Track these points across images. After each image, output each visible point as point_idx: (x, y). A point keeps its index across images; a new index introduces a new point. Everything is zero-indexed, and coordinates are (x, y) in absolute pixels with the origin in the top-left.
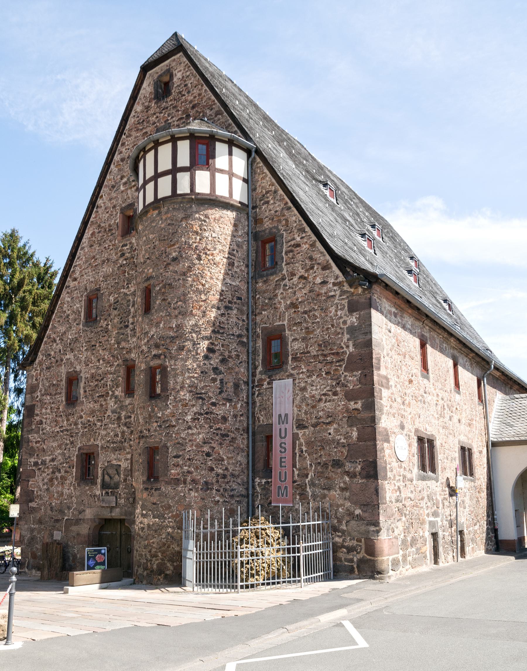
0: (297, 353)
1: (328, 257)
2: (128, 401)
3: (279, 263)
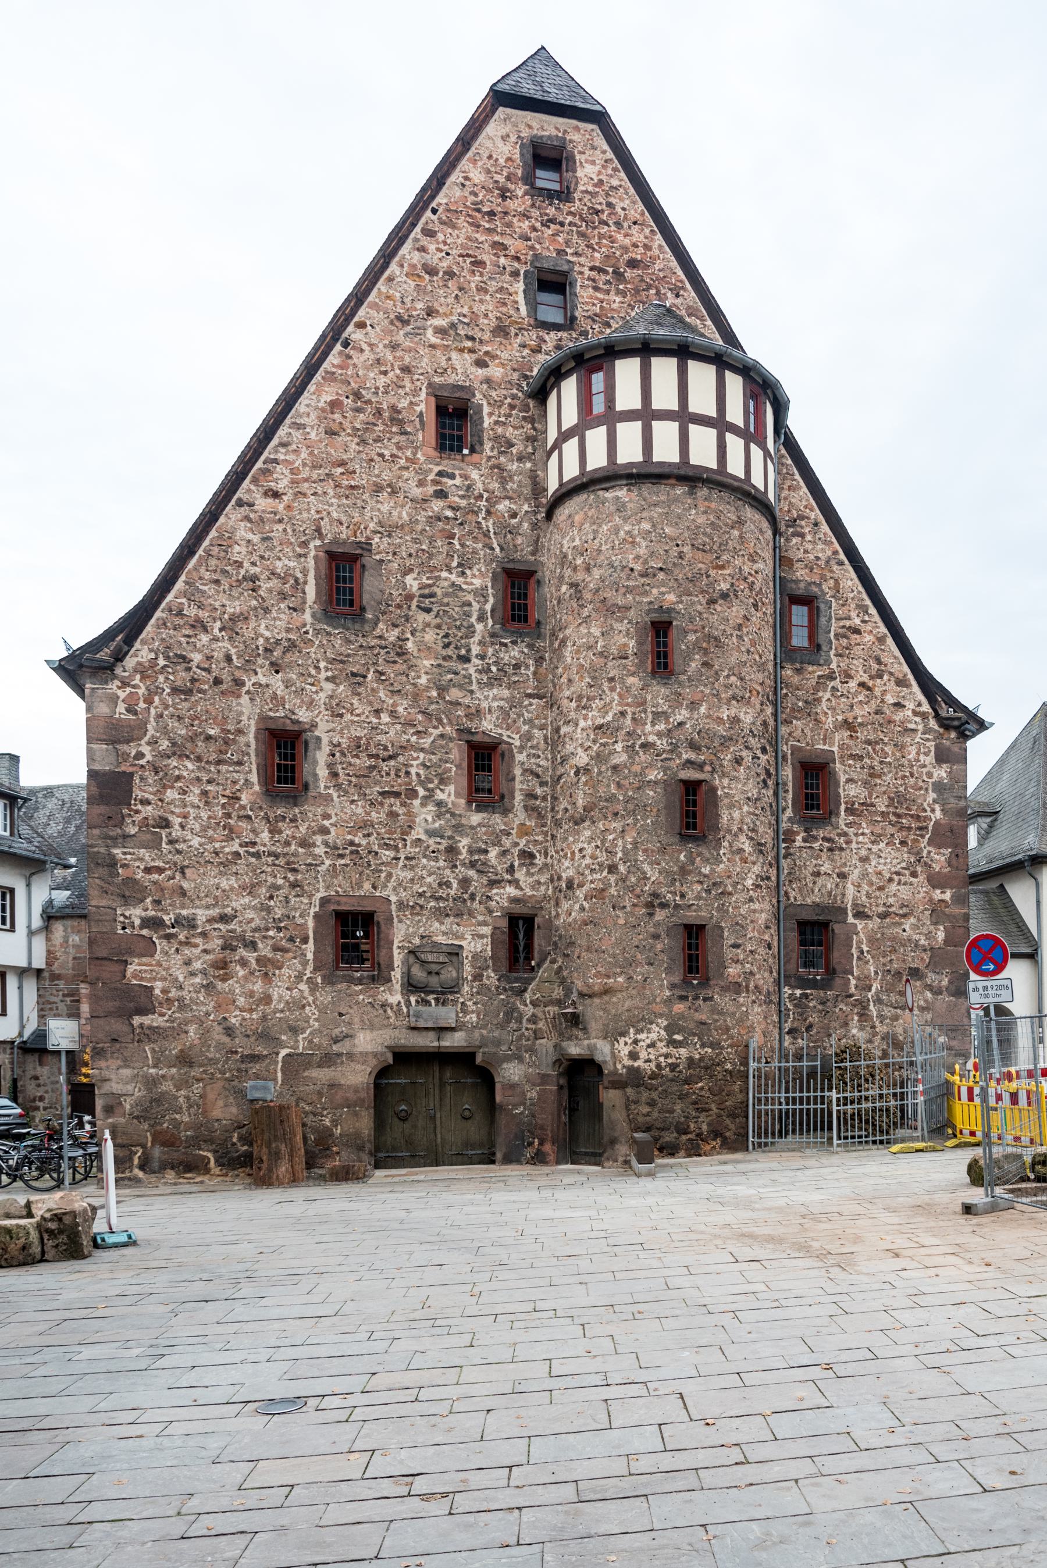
0: (853, 803)
1: (906, 669)
2: (476, 818)
3: (824, 648)
